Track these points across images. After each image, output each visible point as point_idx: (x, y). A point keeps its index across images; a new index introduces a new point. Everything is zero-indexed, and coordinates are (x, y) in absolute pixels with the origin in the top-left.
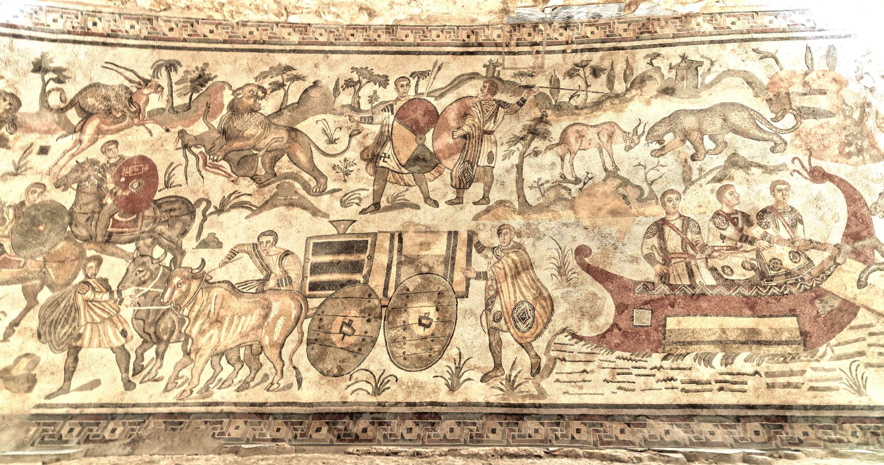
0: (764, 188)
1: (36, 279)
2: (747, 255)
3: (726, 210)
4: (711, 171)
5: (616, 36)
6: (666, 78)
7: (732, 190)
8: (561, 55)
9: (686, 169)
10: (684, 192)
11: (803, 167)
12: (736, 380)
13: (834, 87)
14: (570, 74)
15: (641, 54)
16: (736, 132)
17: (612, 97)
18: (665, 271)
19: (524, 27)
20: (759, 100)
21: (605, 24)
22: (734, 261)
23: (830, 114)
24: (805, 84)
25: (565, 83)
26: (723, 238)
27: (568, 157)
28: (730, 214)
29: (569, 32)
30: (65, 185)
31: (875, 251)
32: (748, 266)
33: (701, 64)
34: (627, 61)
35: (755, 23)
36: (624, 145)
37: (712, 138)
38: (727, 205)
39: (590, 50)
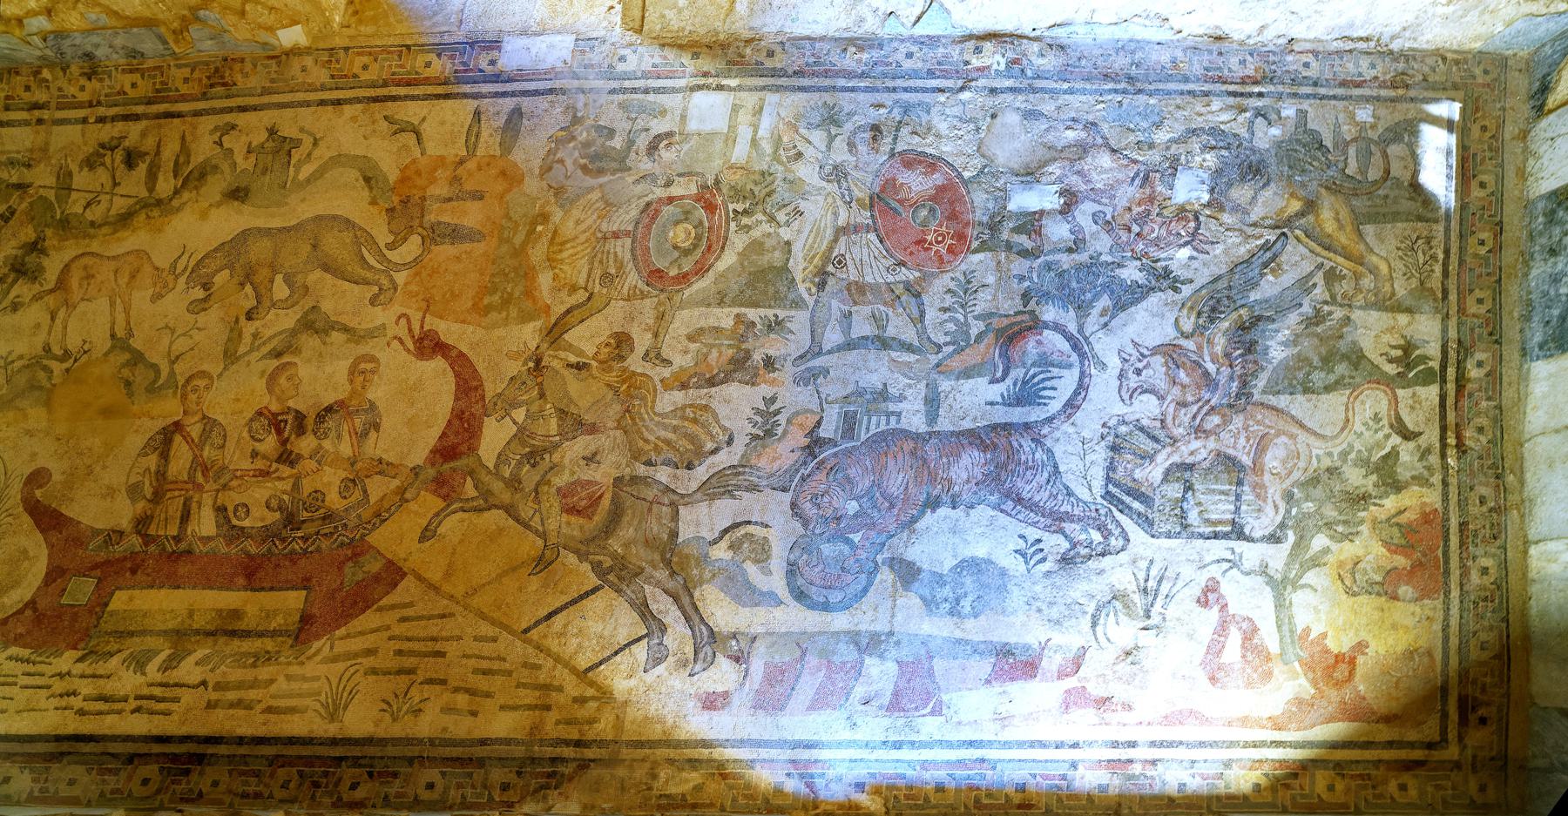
0: (343, 367)
2: (280, 485)
3: (275, 407)
4: (271, 338)
5: (170, 90)
6: (238, 170)
7: (292, 371)
8: (79, 127)
9: (236, 333)
10: (220, 375)
11: (410, 330)
12: (166, 695)
13: (499, 187)
14: (90, 163)
15: (208, 123)
16: (326, 268)
17: (150, 205)
18: (149, 513)
19: (17, 73)
20: (375, 210)
21: (156, 68)
22: (257, 495)
23: (473, 236)
24: (455, 180)
25: (81, 179)
26: (255, 454)
27: (61, 314)
28: (278, 414)
29: (94, 84)
31: (469, 479)
32: (274, 503)
33: (297, 143)
34: (183, 138)
35: (402, 66)
36: (150, 292)
37: (288, 281)
38: (278, 399)
39: (126, 118)
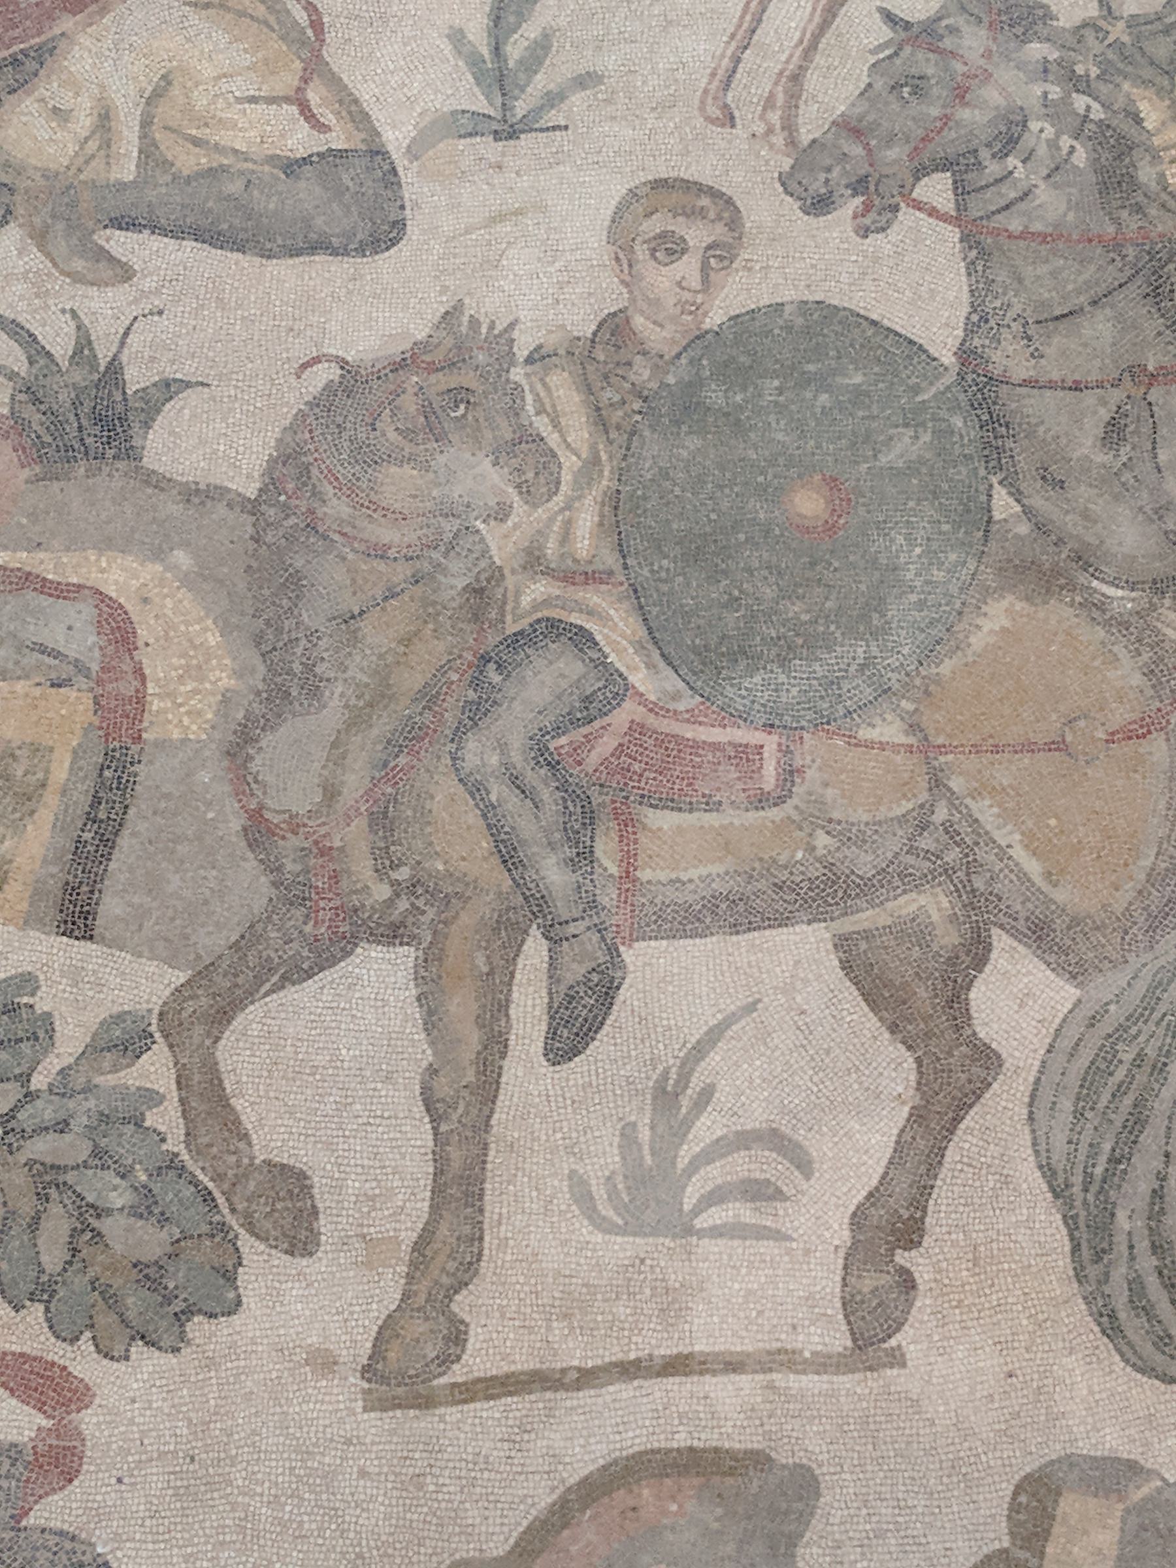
1: (910, 881)
30: (859, 185)
